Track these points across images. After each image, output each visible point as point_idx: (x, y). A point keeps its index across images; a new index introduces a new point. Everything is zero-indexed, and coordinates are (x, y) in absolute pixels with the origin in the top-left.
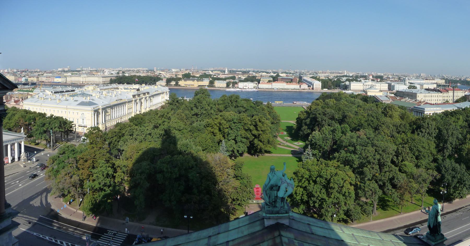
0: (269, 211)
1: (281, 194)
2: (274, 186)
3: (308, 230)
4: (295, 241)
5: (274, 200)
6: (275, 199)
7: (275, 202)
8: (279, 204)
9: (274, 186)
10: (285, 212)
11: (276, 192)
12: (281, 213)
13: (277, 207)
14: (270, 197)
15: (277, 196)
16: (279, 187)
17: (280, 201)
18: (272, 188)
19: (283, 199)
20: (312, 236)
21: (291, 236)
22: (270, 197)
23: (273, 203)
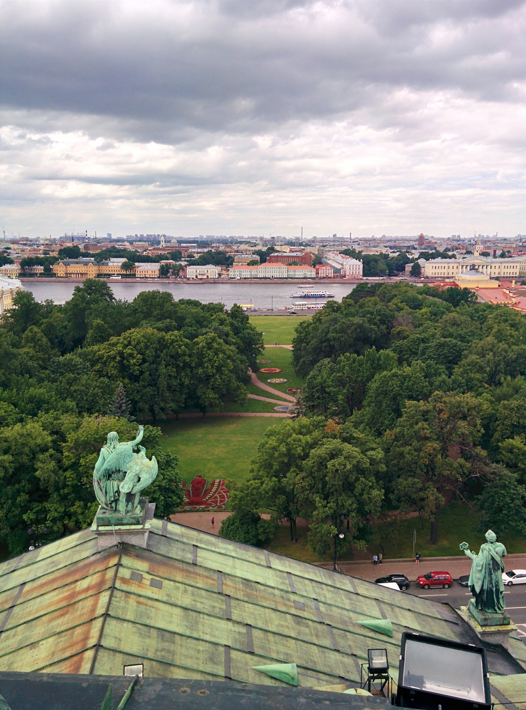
0: (103, 519)
1: (125, 487)
2: (113, 473)
3: (189, 557)
4: (146, 575)
5: (112, 499)
6: (114, 496)
7: (116, 501)
8: (122, 506)
9: (113, 473)
11: (115, 483)
12: (127, 524)
13: (119, 511)
14: (106, 493)
15: (118, 492)
16: (126, 472)
17: (124, 500)
19: (130, 496)
20: (191, 569)
21: (142, 566)
22: (106, 493)
23: (114, 505)
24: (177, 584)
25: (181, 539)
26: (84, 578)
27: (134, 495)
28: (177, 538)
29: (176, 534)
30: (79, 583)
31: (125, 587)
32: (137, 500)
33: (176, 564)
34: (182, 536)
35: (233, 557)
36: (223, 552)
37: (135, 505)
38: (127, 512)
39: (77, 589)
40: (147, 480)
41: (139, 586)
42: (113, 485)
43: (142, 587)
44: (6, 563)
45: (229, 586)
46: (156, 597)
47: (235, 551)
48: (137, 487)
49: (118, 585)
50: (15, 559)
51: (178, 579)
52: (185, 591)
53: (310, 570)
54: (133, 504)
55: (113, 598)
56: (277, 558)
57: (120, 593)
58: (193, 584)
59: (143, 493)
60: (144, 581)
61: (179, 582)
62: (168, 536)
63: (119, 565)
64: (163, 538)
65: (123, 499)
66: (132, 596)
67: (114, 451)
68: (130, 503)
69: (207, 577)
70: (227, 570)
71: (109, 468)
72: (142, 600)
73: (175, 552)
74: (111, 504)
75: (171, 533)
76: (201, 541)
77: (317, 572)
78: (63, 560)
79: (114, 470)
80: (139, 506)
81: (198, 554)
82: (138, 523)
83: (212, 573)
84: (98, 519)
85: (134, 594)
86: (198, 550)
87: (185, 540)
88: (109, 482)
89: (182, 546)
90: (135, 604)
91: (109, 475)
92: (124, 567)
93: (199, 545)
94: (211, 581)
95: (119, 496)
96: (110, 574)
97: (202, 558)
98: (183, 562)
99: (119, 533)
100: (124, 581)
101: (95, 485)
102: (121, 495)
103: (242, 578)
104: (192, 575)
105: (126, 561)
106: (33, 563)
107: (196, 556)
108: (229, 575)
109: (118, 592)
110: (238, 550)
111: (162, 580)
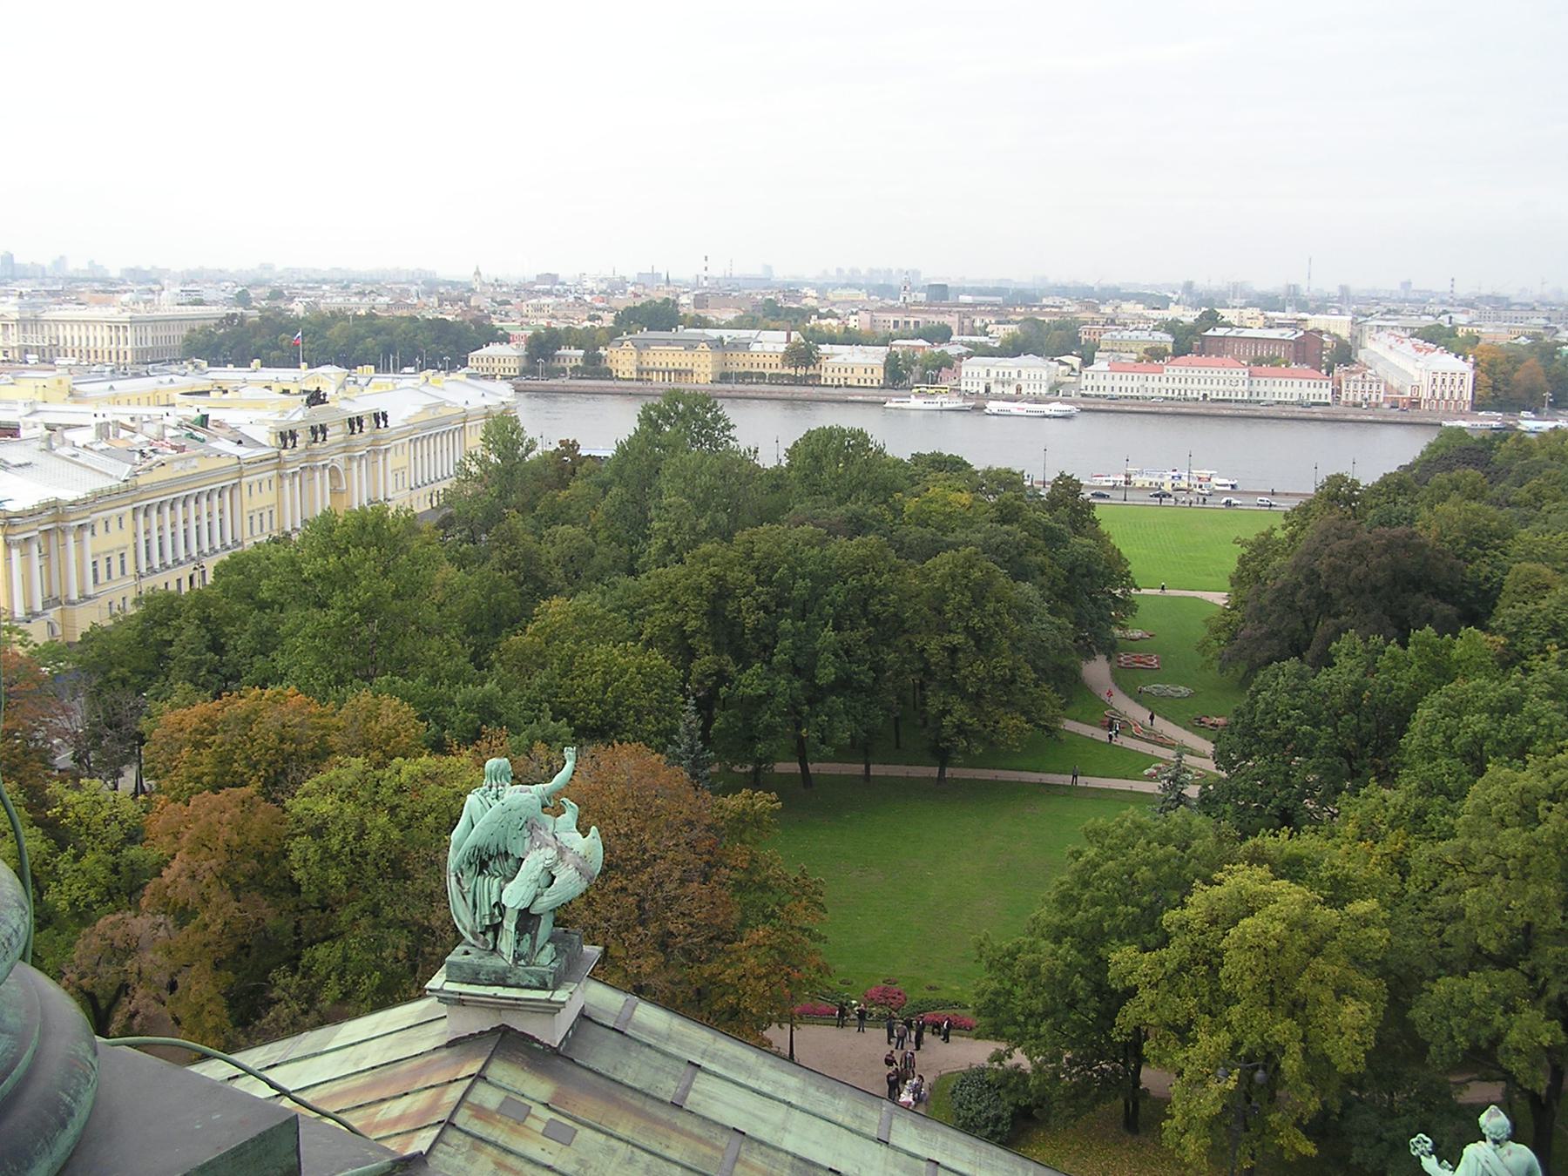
0: (459, 966)
1: (515, 895)
3: (668, 1088)
6: (492, 915)
7: (496, 928)
8: (507, 943)
10: (535, 982)
12: (518, 986)
14: (475, 906)
17: (513, 929)
18: (484, 865)
19: (527, 919)
20: (663, 1113)
21: (536, 1087)
22: (475, 906)
23: (490, 936)
24: (614, 1142)
25: (662, 1046)
26: (400, 1097)
27: (538, 917)
28: (652, 1041)
29: (652, 1032)
30: (386, 1105)
31: (477, 1127)
32: (545, 928)
33: (628, 1097)
34: (669, 1038)
35: (789, 1104)
36: (766, 1089)
37: (540, 942)
38: (518, 957)
39: (378, 1118)
40: (569, 883)
41: (513, 1130)
42: (488, 886)
43: (521, 1134)
44: (266, 1048)
45: (753, 1168)
46: (549, 1160)
47: (803, 1092)
48: (545, 899)
49: (461, 1119)
50: (287, 1041)
51: (621, 1131)
52: (631, 1161)
53: (1000, 1163)
54: (534, 938)
55: (440, 1146)
56: (913, 1122)
57: (462, 1136)
58: (657, 1148)
59: (563, 916)
60: (530, 1121)
61: (620, 1139)
62: (629, 1031)
63: (480, 1077)
64: (614, 1034)
65: (510, 924)
66: (490, 1149)
67: (490, 804)
68: (527, 936)
69: (699, 1139)
70: (763, 1133)
71: (480, 844)
72: (511, 1160)
73: (633, 1071)
74: (484, 933)
75: (640, 1027)
76: (713, 1058)
77: (1020, 1171)
78: (374, 1055)
79: (493, 850)
80: (550, 947)
81: (695, 1085)
82: (543, 986)
83: (716, 1131)
84: (452, 964)
85: (495, 1145)
86: (700, 1074)
87: (672, 1049)
88: (480, 878)
89: (659, 1060)
90: (492, 1166)
91: (482, 861)
92: (490, 1083)
93: (704, 1064)
94: (708, 1150)
95: (502, 915)
96: (455, 1092)
97: (701, 1093)
98: (647, 1095)
99: (499, 1005)
100: (480, 1112)
101: (452, 882)
102: (508, 913)
103: (795, 1156)
104: (661, 1129)
105: (498, 1071)
106: (316, 1055)
107: (688, 1088)
108: (762, 1143)
109: (457, 1133)
110: (811, 1090)
111: (577, 1126)
